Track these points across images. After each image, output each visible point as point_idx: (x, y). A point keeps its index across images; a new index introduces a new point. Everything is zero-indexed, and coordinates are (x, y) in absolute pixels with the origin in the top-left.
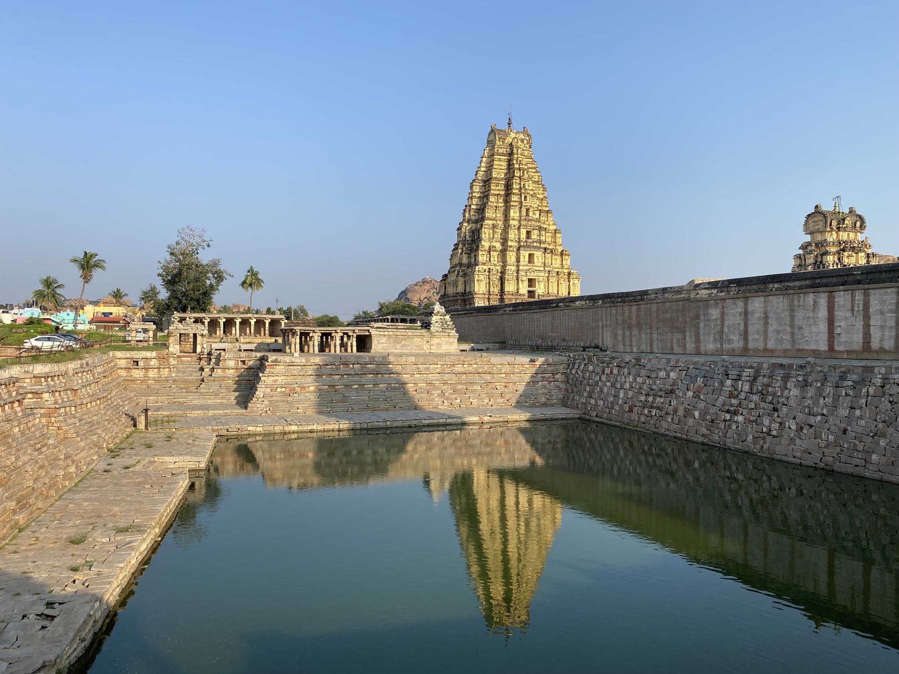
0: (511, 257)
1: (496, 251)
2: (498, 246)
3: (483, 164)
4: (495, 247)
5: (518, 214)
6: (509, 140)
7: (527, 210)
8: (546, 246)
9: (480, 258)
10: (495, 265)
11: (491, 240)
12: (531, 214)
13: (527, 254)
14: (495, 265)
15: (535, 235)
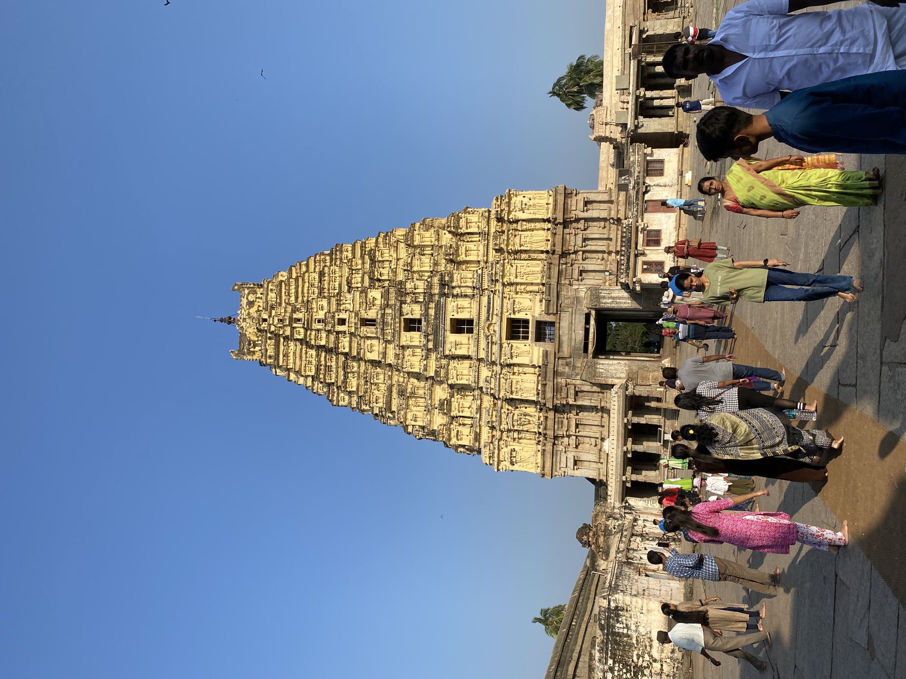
0: (462, 373)
1: (449, 403)
2: (441, 393)
3: (301, 381)
4: (442, 404)
5: (375, 342)
6: (251, 332)
7: (366, 322)
8: (436, 280)
9: (467, 441)
10: (479, 409)
11: (429, 410)
12: (372, 314)
13: (452, 338)
14: (479, 409)
15: (416, 312)
